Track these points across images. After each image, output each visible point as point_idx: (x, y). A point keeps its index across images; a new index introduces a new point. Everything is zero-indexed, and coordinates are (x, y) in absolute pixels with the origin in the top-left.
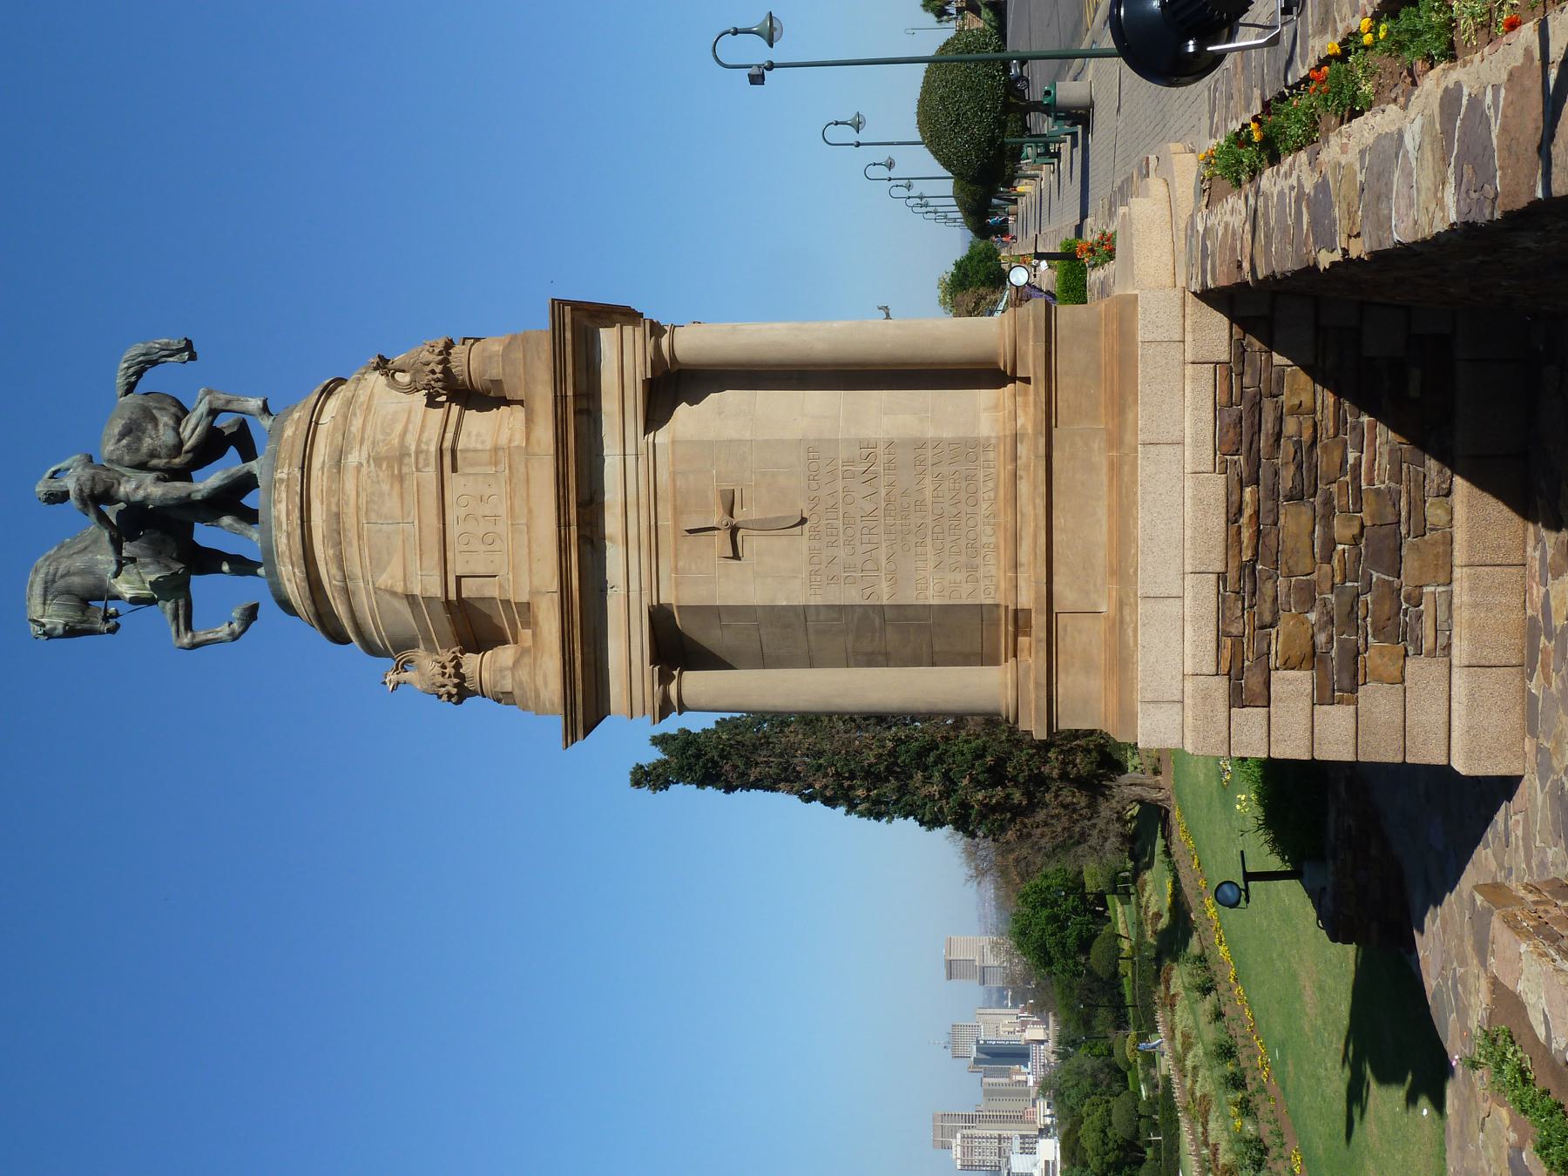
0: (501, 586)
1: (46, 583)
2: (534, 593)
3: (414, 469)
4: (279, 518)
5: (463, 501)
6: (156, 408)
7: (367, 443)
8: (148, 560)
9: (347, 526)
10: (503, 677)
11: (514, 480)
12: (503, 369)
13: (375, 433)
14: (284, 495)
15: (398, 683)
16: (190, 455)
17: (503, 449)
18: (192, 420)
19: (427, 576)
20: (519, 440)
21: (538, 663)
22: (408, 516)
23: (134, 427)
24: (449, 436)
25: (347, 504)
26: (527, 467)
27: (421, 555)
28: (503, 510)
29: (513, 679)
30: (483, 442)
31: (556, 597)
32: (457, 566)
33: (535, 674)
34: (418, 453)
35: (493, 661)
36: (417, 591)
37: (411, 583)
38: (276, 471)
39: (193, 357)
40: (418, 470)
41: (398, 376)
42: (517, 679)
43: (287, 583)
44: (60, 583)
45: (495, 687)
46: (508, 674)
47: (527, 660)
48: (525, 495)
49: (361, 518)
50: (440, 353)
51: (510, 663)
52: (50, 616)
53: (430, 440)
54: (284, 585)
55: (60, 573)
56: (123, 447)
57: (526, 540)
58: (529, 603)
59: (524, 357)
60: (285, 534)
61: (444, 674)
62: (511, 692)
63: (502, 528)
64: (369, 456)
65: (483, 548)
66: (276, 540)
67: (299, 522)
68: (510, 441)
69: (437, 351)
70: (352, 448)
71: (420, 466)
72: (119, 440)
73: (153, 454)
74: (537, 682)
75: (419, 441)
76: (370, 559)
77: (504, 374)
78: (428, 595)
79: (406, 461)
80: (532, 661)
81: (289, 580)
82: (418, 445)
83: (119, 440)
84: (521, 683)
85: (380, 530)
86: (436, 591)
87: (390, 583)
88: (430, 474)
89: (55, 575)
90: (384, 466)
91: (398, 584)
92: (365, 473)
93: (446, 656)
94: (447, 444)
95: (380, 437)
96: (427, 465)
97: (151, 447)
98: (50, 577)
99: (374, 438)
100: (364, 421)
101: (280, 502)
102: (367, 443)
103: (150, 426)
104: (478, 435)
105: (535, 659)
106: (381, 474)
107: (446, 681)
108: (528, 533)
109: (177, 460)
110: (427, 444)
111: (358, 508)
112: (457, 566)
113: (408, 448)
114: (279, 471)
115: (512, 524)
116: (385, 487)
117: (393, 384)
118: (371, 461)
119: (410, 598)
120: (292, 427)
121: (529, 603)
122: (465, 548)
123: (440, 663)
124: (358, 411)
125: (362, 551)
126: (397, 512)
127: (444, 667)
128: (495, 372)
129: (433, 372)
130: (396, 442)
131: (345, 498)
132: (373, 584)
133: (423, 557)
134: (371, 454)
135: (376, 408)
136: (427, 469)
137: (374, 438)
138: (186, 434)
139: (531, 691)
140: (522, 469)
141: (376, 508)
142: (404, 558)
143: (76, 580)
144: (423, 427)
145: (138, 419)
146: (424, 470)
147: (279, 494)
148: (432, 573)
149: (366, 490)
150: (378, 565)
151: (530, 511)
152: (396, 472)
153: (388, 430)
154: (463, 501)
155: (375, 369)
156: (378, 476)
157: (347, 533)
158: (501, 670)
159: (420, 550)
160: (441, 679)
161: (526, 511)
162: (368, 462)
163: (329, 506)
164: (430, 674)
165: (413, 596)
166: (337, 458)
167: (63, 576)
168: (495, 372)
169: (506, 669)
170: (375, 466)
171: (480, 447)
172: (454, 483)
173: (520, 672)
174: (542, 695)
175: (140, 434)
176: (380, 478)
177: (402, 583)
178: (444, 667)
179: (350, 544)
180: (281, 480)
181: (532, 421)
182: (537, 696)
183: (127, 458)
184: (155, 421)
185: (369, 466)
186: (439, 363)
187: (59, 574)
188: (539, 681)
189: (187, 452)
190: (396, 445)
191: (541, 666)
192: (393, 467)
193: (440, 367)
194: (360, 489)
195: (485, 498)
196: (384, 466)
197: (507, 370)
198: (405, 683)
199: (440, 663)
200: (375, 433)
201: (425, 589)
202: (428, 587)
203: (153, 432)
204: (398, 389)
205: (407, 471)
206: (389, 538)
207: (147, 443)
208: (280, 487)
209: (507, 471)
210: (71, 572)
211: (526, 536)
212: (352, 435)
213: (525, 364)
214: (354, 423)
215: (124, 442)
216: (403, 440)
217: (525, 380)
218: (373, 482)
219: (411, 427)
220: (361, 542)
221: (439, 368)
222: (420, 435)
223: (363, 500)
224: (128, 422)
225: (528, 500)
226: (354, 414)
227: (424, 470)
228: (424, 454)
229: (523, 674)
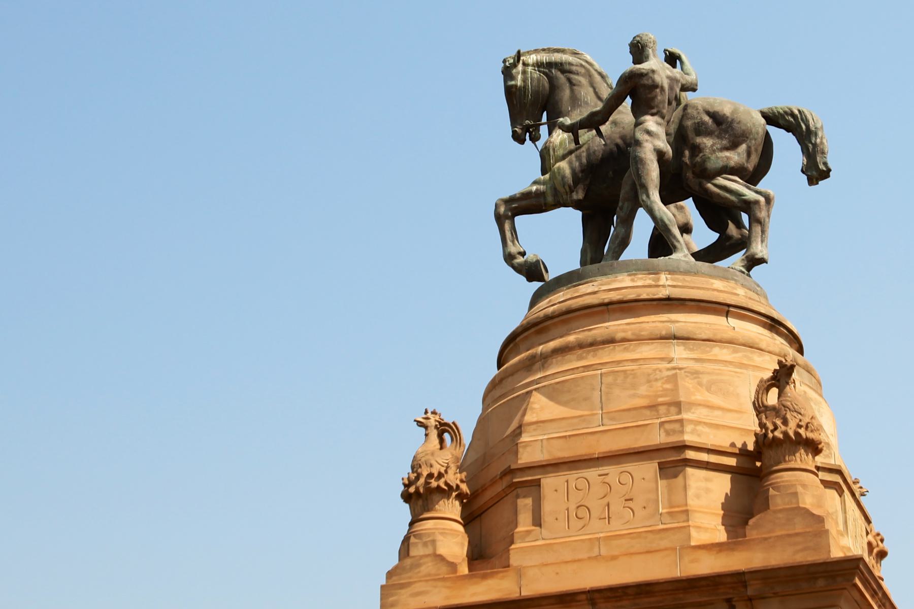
0: (528, 532)
1: (561, 64)
2: (520, 573)
3: (663, 420)
4: (615, 281)
5: (626, 478)
6: (749, 148)
7: (697, 366)
8: (584, 160)
9: (600, 352)
10: (425, 544)
11: (650, 536)
12: (781, 511)
13: (709, 373)
14: (640, 283)
15: (426, 427)
16: (697, 188)
17: (688, 521)
18: (737, 185)
19: (542, 447)
20: (698, 538)
21: (440, 584)
22: (612, 419)
23: (724, 126)
24: (704, 457)
25: (626, 349)
26: (666, 549)
27: (565, 437)
28: (617, 527)
29: (422, 557)
30: (698, 496)
31: (515, 595)
32: (550, 483)
33: (427, 581)
34: (681, 421)
35: (444, 533)
36: (525, 438)
37: (535, 430)
38: (669, 274)
39: (812, 181)
40: (662, 424)
41: (774, 391)
42: (421, 561)
43: (548, 300)
44: (562, 78)
45: (415, 536)
46: (429, 550)
47: (444, 570)
48: (632, 551)
49: (608, 366)
50: (797, 434)
51: (442, 550)
52: (524, 72)
53: (699, 435)
54: (547, 298)
55: (572, 76)
56: (701, 119)
57: (581, 556)
58: (508, 566)
59: (797, 534)
60: (596, 289)
61: (430, 476)
62: (408, 554)
63: (598, 529)
64: (680, 369)
65: (572, 507)
66: (591, 281)
67: (606, 301)
68: (698, 528)
69: (802, 431)
70: (691, 350)
71: (667, 426)
72: (708, 113)
73: (696, 149)
74: (417, 585)
75: (698, 423)
76: (563, 381)
77: (775, 512)
78: (520, 450)
79: (673, 409)
80: (442, 576)
81: (550, 301)
82: (691, 421)
83: (708, 113)
84: (418, 565)
85: (593, 389)
86: (526, 457)
87: (536, 406)
88: (658, 438)
89: (571, 72)
90: (668, 386)
91: (535, 415)
92: (660, 366)
93: (454, 478)
94: (691, 455)
95: (705, 379)
96: (668, 433)
97: (702, 146)
98: (567, 67)
99: (702, 373)
100: (726, 361)
101: (633, 280)
102: (697, 366)
103: (725, 142)
104: (708, 491)
105: (444, 579)
106: (659, 384)
107: (422, 481)
108: (589, 558)
109: (689, 175)
110: (693, 432)
111: (619, 362)
112: (550, 483)
113: (689, 410)
114: (669, 276)
115: (598, 539)
116: (643, 390)
117: (765, 387)
118: (674, 372)
119: (518, 431)
120: (724, 287)
121: (508, 566)
122: (572, 485)
123: (446, 472)
124: (739, 355)
125: (571, 372)
126: (614, 406)
127: (440, 476)
128: (777, 500)
129: (776, 428)
130: (698, 397)
131: (632, 347)
132: (535, 389)
133: (564, 440)
134: (683, 371)
135: (741, 373)
136: (663, 434)
137: (702, 373)
138: (720, 181)
139: (410, 578)
140: (664, 543)
141: (618, 381)
142: (563, 419)
143: (566, 93)
144: (717, 426)
145: (733, 129)
146: (662, 430)
147: (641, 279)
148: (545, 451)
149: (640, 368)
150: (553, 393)
151: (614, 558)
152: (660, 400)
153: (713, 388)
154: (626, 478)
155: (780, 363)
156: (656, 380)
157: (592, 353)
158: (434, 542)
159: (570, 436)
160: (425, 473)
161: (616, 553)
162: (674, 368)
163: (624, 331)
164: (433, 462)
165: (520, 434)
166: (678, 334)
167: (569, 80)
168: (779, 501)
169: (435, 549)
170: (668, 376)
171: (691, 493)
172: (648, 469)
173: (430, 564)
174: (403, 591)
175: (716, 133)
176: (654, 383)
177: (535, 420)
178: (440, 476)
179: (580, 358)
180: (658, 279)
181: (720, 551)
182: (403, 586)
183: (689, 123)
184: (733, 146)
185: (668, 369)
186: (785, 434)
187: (572, 76)
188: (418, 587)
189: (701, 186)
190: (693, 398)
191: (435, 587)
192: (665, 396)
193: (781, 436)
194: (641, 362)
195: (630, 504)
196: (668, 386)
197: (780, 515)
198: (426, 435)
199: (446, 472)
200: (709, 373)
201: (525, 447)
202: (529, 449)
203: (719, 146)
204: (757, 392)
205: (661, 412)
206: (586, 399)
207: (707, 142)
208: (650, 279)
209: (661, 527)
210: (575, 88)
211: (584, 555)
212: (708, 349)
213: (789, 536)
214: (725, 351)
215: (706, 118)
216: (700, 405)
217: (770, 538)
218: (649, 375)
219: (718, 413)
220: (581, 369)
221: (778, 434)
222: (704, 423)
223: (629, 367)
224: (730, 120)
225: (626, 555)
226: (735, 351)
227: (662, 430)
228: (681, 429)
229: (428, 567)
